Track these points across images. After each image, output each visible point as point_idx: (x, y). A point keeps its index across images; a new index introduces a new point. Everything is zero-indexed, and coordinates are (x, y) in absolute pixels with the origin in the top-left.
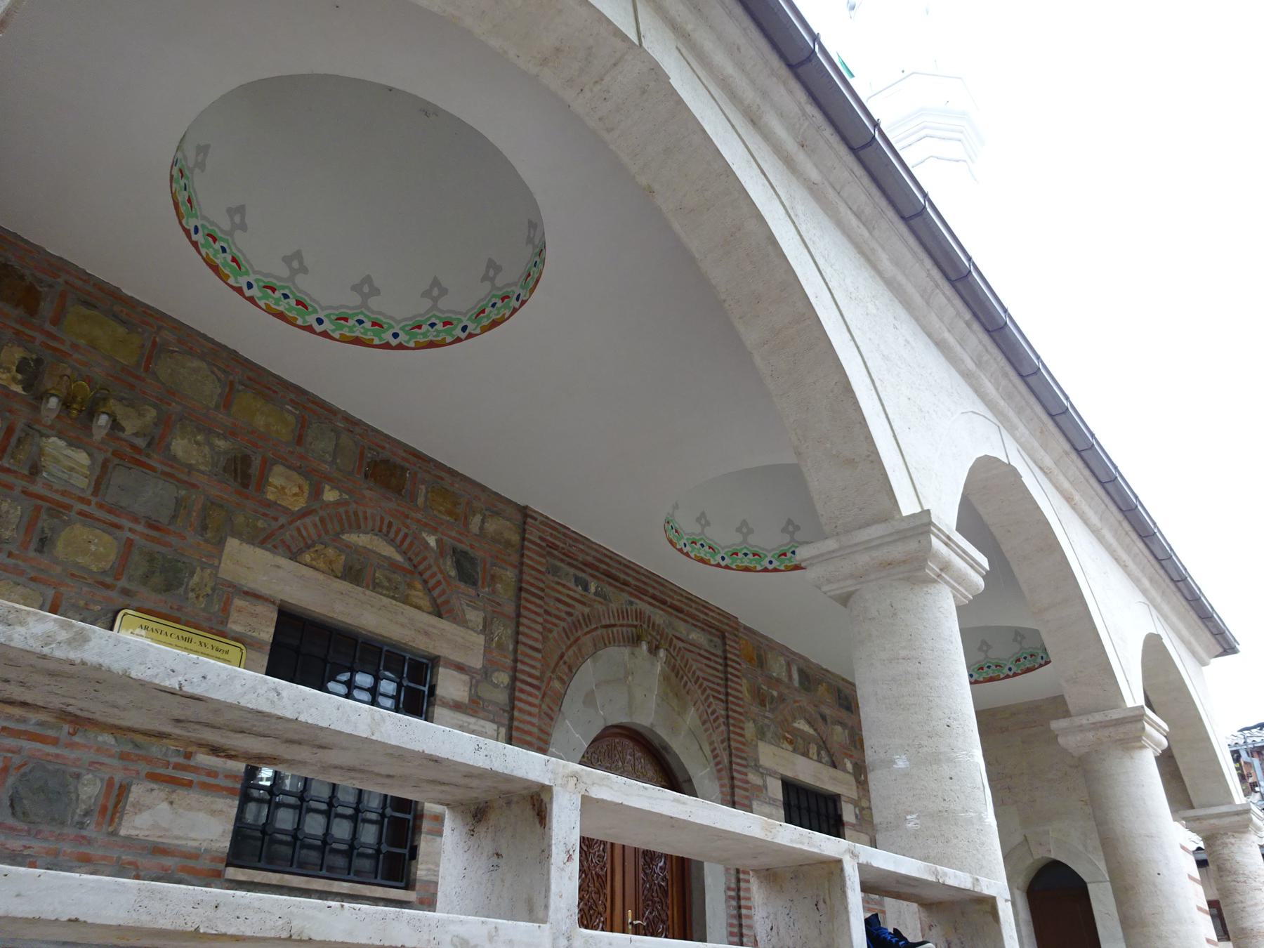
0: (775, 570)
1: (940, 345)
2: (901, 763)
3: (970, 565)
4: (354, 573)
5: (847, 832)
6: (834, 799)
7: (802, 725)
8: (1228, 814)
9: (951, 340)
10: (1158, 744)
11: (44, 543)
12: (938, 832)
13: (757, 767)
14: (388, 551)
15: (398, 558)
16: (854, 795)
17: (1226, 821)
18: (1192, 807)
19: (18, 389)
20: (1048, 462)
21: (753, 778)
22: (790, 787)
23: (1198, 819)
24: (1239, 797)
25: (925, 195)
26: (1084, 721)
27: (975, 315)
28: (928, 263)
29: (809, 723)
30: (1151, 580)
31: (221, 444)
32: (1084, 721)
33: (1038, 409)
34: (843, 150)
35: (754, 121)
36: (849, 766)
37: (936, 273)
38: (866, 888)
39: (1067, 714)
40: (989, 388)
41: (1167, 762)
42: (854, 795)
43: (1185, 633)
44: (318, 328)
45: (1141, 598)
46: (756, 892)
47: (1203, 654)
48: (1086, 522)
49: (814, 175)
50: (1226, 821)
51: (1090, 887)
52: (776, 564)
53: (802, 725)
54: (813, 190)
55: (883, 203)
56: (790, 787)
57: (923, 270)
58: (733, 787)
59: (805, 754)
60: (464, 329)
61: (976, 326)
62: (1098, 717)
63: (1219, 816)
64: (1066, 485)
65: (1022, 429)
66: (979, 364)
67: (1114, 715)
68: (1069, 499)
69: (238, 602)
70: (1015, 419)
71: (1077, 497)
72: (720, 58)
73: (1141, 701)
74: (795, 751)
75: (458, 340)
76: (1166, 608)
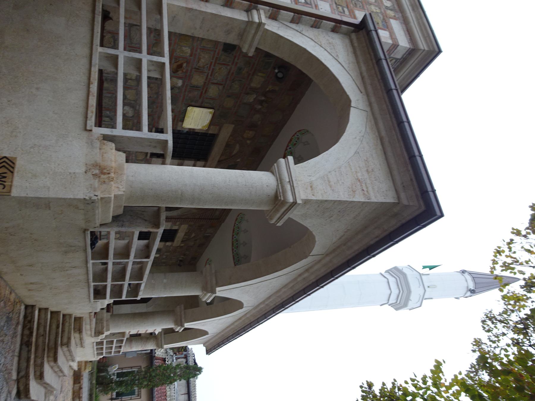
0: (233, 238)
1: (269, 298)
2: (165, 281)
3: (208, 298)
4: (228, 145)
5: (163, 243)
6: (172, 240)
7: (193, 235)
8: (161, 343)
9: (271, 300)
10: (176, 329)
11: (229, 96)
12: (151, 286)
13: (181, 224)
14: (235, 152)
15: (233, 154)
16: (174, 245)
17: (160, 342)
18: (165, 334)
19: (268, 89)
20: (248, 316)
21: (178, 223)
22: (176, 231)
23: (161, 335)
24: (166, 346)
25: (298, 302)
26: (183, 313)
27: (277, 306)
28: (286, 299)
29: (194, 237)
30: (223, 335)
31: (259, 123)
32: (183, 313)
33: (259, 316)
34: (304, 287)
35: (307, 270)
36: (182, 245)
37: (284, 300)
38: (138, 284)
39: (185, 309)
40: (262, 306)
41: (172, 331)
42: (174, 245)
43: (211, 341)
44: (288, 148)
45: (219, 332)
46: (139, 266)
47: (206, 345)
48: (236, 322)
49: (299, 279)
50: (160, 342)
51: (145, 304)
52: (234, 239)
53: (193, 235)
54: (295, 279)
55: (297, 292)
56: (176, 231)
57: (285, 297)
58: (175, 219)
59: (185, 235)
61: (274, 306)
62: (183, 316)
63: (161, 340)
64: (243, 319)
65: (254, 311)
66: (267, 305)
67: (183, 320)
68: (240, 319)
69: (218, 127)
70: (257, 310)
71: (241, 321)
72: (316, 268)
73: (186, 327)
74: (186, 233)
76: (217, 337)
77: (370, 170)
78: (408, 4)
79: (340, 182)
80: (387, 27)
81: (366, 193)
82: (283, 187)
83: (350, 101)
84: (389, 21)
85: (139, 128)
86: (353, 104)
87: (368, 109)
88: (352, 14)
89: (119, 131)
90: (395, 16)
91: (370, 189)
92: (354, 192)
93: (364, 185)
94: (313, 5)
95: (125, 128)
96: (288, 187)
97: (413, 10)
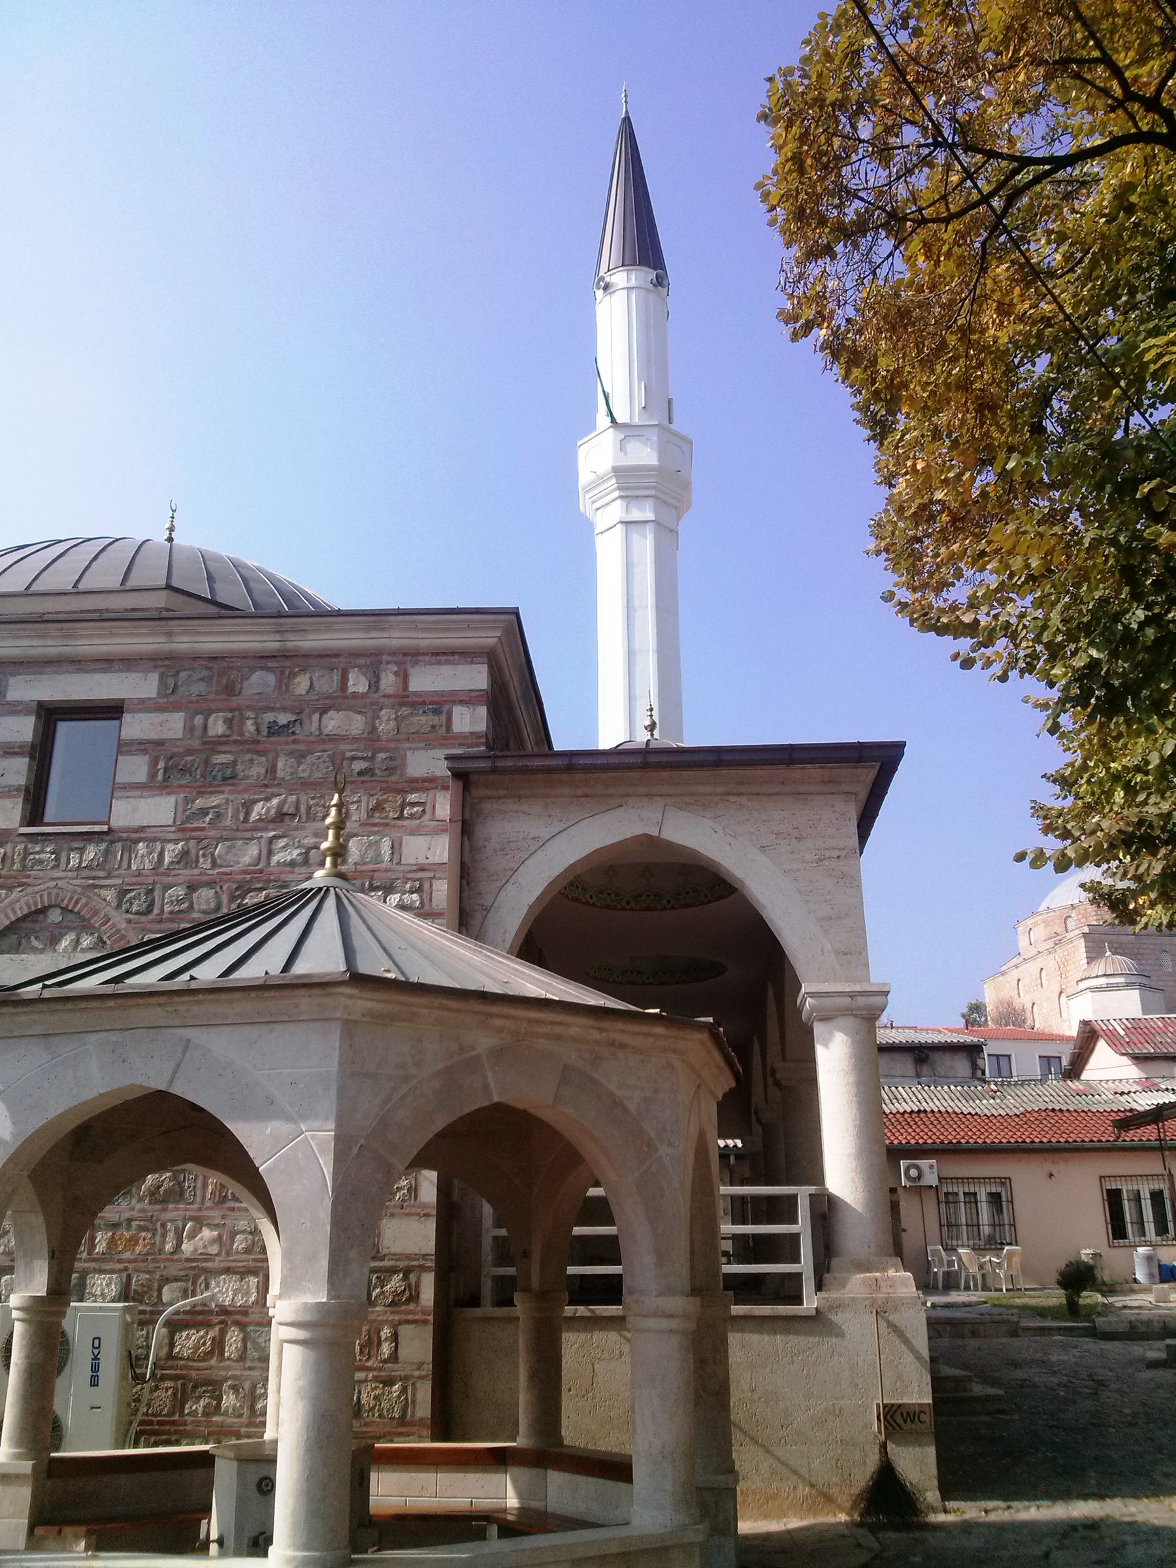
18: (750, 1134)
60: (628, 903)
75: (623, 909)
77: (795, 833)
78: (361, 635)
79: (829, 897)
80: (440, 704)
81: (843, 853)
82: (859, 1009)
83: (647, 836)
84: (415, 694)
85: (795, 1237)
86: (653, 831)
87: (660, 802)
88: (419, 785)
89: (805, 1265)
90: (396, 674)
91: (834, 843)
92: (844, 875)
93: (828, 854)
94: (420, 875)
95: (796, 1259)
96: (861, 1001)
97: (383, 630)
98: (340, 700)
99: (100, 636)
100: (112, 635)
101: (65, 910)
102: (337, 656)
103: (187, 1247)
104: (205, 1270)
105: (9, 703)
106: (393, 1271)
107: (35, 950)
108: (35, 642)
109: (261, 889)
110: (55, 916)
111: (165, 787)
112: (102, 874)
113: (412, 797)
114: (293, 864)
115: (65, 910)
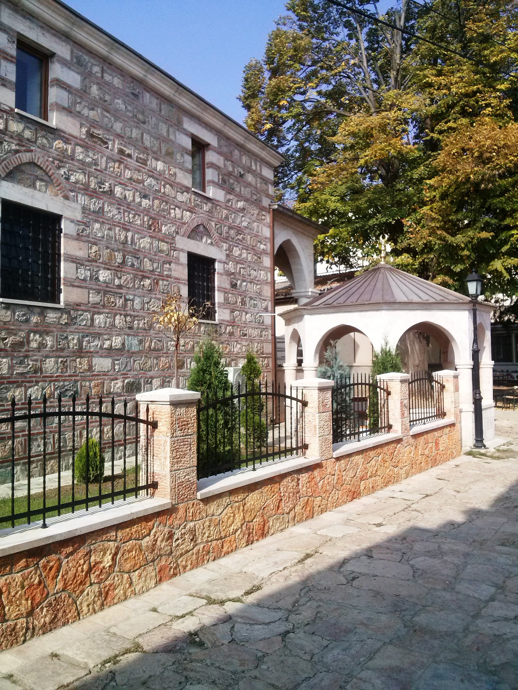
98: (249, 170)
99: (211, 115)
100: (214, 117)
101: (204, 227)
102: (249, 152)
103: (235, 350)
104: (239, 357)
105: (184, 129)
106: (265, 357)
107: (196, 240)
108: (195, 107)
109: (241, 234)
110: (201, 228)
111: (221, 187)
112: (211, 215)
113: (264, 213)
114: (246, 227)
115: (204, 227)
